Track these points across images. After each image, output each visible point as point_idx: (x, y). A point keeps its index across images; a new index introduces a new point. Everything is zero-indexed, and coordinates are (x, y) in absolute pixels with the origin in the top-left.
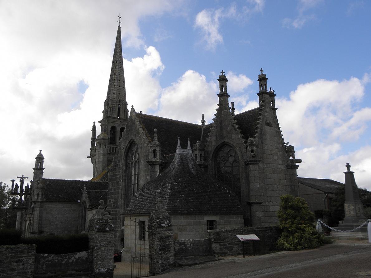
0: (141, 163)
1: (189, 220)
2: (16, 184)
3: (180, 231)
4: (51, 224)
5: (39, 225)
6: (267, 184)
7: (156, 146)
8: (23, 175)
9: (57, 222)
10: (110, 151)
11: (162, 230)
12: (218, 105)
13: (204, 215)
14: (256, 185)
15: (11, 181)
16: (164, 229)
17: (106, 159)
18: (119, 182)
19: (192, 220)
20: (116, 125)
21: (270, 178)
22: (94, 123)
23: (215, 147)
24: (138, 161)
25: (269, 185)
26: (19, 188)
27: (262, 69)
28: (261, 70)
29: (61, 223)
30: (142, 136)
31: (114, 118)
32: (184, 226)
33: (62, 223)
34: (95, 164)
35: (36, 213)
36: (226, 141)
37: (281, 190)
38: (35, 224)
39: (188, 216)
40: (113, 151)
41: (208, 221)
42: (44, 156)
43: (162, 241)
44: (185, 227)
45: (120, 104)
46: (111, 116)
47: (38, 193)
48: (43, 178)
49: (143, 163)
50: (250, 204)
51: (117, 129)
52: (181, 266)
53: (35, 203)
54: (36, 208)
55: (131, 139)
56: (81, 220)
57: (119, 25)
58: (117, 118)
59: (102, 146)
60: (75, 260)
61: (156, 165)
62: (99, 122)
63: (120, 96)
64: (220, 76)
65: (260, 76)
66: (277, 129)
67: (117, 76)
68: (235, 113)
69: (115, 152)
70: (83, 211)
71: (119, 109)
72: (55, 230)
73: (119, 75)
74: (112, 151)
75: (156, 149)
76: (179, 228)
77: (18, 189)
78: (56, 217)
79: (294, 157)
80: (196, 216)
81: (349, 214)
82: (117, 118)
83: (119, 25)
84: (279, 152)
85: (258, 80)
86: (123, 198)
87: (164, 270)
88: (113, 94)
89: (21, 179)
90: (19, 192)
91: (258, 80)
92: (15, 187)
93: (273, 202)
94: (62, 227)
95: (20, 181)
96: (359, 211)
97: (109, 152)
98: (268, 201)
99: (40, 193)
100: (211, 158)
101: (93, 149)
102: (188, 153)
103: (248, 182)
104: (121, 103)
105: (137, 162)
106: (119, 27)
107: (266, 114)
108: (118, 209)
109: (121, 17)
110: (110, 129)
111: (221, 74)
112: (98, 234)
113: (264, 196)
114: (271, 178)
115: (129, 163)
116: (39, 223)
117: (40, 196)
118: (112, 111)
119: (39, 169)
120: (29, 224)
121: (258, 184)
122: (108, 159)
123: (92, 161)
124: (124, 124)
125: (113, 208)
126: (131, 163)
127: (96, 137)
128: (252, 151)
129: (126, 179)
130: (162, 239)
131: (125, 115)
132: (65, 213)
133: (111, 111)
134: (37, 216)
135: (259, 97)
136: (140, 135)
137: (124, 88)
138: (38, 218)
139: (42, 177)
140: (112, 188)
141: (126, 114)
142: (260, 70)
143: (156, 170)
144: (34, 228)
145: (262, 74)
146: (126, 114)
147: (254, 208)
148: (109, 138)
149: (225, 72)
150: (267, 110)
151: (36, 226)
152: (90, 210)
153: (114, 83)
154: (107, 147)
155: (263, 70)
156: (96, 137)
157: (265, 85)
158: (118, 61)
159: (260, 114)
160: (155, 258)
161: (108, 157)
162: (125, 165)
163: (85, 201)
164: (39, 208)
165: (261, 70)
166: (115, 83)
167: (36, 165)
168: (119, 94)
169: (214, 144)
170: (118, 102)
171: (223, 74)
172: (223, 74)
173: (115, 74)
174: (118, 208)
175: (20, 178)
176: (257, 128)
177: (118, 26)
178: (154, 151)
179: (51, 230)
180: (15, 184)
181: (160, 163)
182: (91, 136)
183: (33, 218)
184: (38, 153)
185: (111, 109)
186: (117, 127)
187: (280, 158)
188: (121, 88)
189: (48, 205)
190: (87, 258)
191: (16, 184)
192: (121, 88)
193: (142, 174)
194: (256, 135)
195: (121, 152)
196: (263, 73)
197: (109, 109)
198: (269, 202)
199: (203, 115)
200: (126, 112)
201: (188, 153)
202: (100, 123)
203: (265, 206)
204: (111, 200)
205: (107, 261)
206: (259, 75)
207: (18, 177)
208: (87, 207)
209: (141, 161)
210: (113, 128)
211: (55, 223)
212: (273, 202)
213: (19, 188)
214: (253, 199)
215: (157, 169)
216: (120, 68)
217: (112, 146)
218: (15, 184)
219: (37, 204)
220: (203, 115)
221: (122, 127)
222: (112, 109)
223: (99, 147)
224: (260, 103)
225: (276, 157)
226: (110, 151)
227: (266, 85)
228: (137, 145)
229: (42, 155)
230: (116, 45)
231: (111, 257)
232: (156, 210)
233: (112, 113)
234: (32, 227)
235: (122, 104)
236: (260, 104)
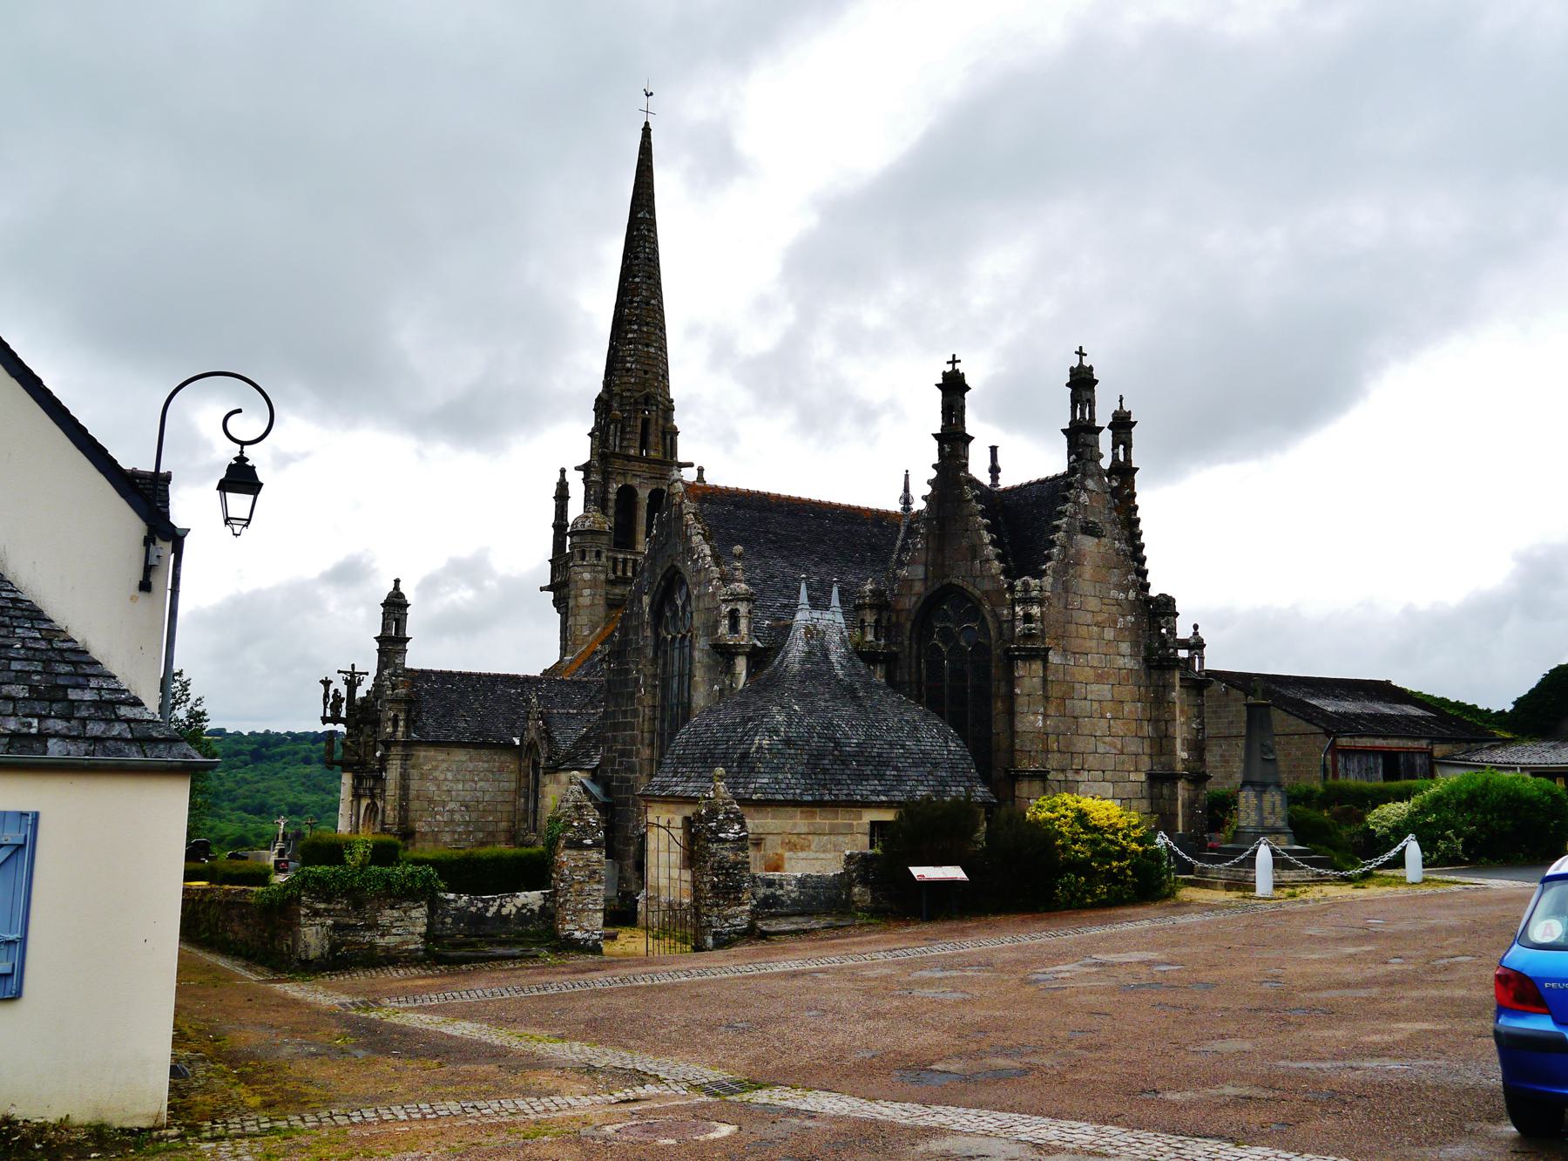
0: (699, 643)
1: (818, 820)
2: (336, 691)
3: (790, 850)
4: (433, 809)
5: (399, 813)
6: (1073, 717)
7: (739, 600)
8: (353, 666)
9: (451, 806)
10: (615, 572)
11: (722, 849)
12: (935, 466)
13: (860, 807)
14: (1032, 721)
15: (322, 682)
16: (728, 845)
17: (600, 601)
18: (634, 693)
19: (827, 822)
20: (635, 482)
21: (1086, 699)
22: (563, 471)
23: (922, 599)
24: (690, 634)
25: (1080, 720)
26: (344, 705)
27: (1081, 348)
28: (1081, 353)
29: (463, 808)
30: (700, 560)
31: (629, 458)
32: (803, 836)
33: (467, 807)
34: (567, 613)
35: (392, 775)
36: (955, 581)
37: (1121, 734)
38: (389, 808)
39: (815, 809)
40: (624, 572)
41: (873, 824)
42: (409, 598)
43: (722, 874)
44: (804, 839)
45: (649, 407)
46: (617, 449)
47: (396, 716)
48: (406, 666)
49: (702, 643)
50: (1015, 777)
52: (764, 936)
53: (388, 745)
54: (390, 762)
55: (669, 565)
56: (522, 800)
58: (639, 459)
59: (587, 554)
60: (514, 910)
61: (738, 654)
62: (577, 469)
63: (648, 379)
64: (944, 373)
65: (1075, 371)
66: (1119, 542)
67: (636, 308)
68: (1000, 482)
69: (630, 574)
70: (531, 774)
71: (646, 422)
72: (447, 829)
73: (644, 306)
74: (619, 573)
75: (738, 607)
76: (787, 841)
77: (341, 706)
78: (448, 791)
79: (1172, 631)
80: (840, 809)
81: (1248, 818)
82: (639, 459)
84: (1123, 616)
85: (1068, 385)
86: (647, 742)
87: (723, 942)
88: (624, 373)
89: (349, 678)
90: (343, 714)
91: (1068, 385)
92: (331, 700)
93: (1089, 771)
94: (468, 819)
95: (347, 682)
96: (1273, 812)
97: (612, 576)
98: (1074, 767)
99: (402, 716)
100: (908, 634)
101: (559, 561)
102: (832, 622)
103: (1011, 713)
104: (652, 405)
105: (686, 642)
106: (647, 131)
107: (1084, 498)
108: (632, 776)
109: (651, 94)
110: (612, 497)
111: (949, 368)
112: (567, 852)
113: (1059, 751)
114: (1089, 698)
115: (665, 638)
116: (401, 806)
117: (401, 723)
118: (623, 431)
119: (392, 642)
120: (368, 805)
121: (1040, 717)
122: (607, 598)
123: (556, 602)
124: (660, 478)
125: (617, 772)
126: (670, 636)
127: (570, 520)
128: (1028, 618)
129: (655, 686)
130: (720, 868)
131: (664, 445)
132: (476, 779)
133: (619, 434)
134: (393, 786)
135: (1069, 441)
136: (696, 556)
137: (661, 350)
138: (398, 792)
139: (404, 664)
140: (614, 711)
141: (668, 441)
142: (1076, 353)
143: (738, 669)
144: (386, 819)
145: (1081, 364)
146: (668, 441)
147: (1023, 789)
148: (610, 528)
149: (959, 361)
150: (1090, 484)
151: (391, 815)
152: (549, 773)
155: (1084, 351)
156: (570, 524)
157: (1089, 401)
158: (642, 256)
159: (1066, 500)
160: (704, 914)
161: (607, 593)
162: (652, 643)
163: (535, 742)
164: (399, 762)
165: (1081, 353)
166: (630, 336)
167: (385, 627)
168: (646, 372)
169: (918, 587)
170: (643, 401)
171: (954, 365)
172: (954, 365)
173: (632, 302)
174: (633, 772)
175: (345, 673)
176: (1052, 544)
177: (643, 125)
178: (734, 616)
179: (436, 829)
180: (331, 693)
181: (748, 650)
182: (552, 518)
183: (384, 791)
184: (390, 587)
185: (619, 425)
186: (638, 489)
187: (1127, 633)
188: (652, 350)
189: (422, 754)
190: (542, 908)
191: (336, 691)
192: (652, 350)
193: (699, 675)
194: (1044, 567)
195: (640, 601)
196: (1086, 363)
197: (612, 427)
198: (1077, 771)
199: (907, 476)
200: (669, 437)
201: (832, 622)
202: (582, 473)
203: (1063, 784)
204: (612, 747)
205: (588, 915)
206: (1072, 369)
207: (339, 672)
208: (543, 761)
209: (696, 638)
210: (627, 494)
211: (447, 808)
212: (1089, 771)
213: (344, 705)
214: (1025, 765)
215: (741, 665)
216: (649, 278)
217: (621, 556)
218: (331, 693)
219: (392, 749)
220: (907, 476)
221: (655, 487)
222: (622, 425)
223: (577, 556)
224: (1069, 458)
225: (1112, 634)
226: (615, 572)
227: (1091, 403)
228: (688, 587)
229: (402, 596)
230: (640, 161)
231: (598, 907)
232: (709, 798)
233: (622, 440)
234: (379, 817)
235: (654, 408)
236: (1069, 463)
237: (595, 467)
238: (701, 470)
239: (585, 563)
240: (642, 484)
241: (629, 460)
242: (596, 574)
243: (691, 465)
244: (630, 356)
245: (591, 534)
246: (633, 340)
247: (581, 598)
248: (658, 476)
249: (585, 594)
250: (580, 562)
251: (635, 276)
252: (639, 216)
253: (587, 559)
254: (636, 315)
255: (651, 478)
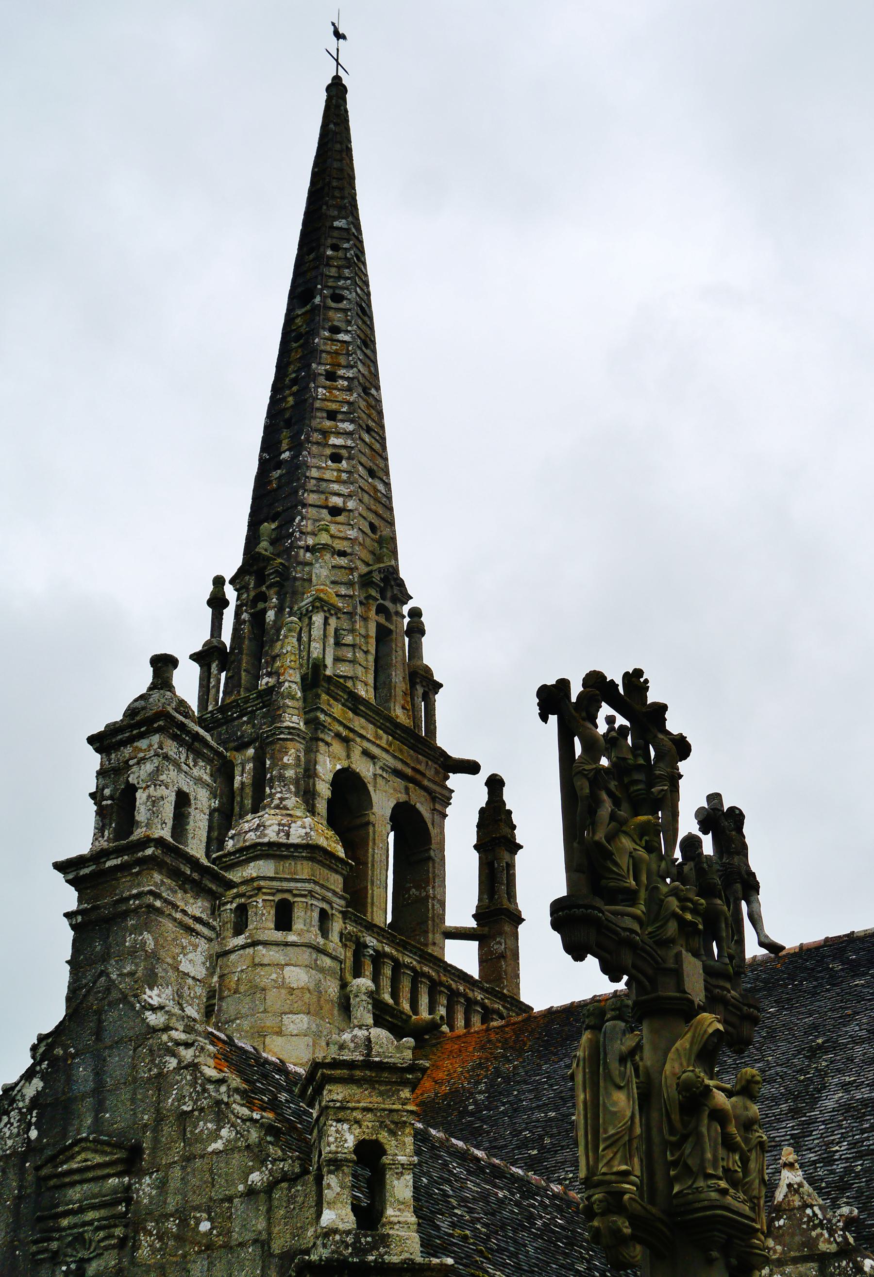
20: (365, 769)
51: (375, 809)
57: (337, 80)
83: (337, 80)
109: (344, 37)
110: (324, 789)
153: (325, 433)
154: (335, 937)
166: (333, 440)
186: (371, 788)
221: (403, 798)
237: (293, 698)
238: (495, 784)
239: (292, 938)
240: (379, 780)
241: (356, 712)
242: (321, 976)
243: (472, 768)
244: (338, 481)
245: (311, 859)
246: (344, 452)
247: (279, 1040)
248: (409, 771)
249: (292, 1028)
250: (279, 936)
251: (335, 330)
252: (336, 224)
253: (298, 925)
254: (349, 403)
255: (397, 773)
